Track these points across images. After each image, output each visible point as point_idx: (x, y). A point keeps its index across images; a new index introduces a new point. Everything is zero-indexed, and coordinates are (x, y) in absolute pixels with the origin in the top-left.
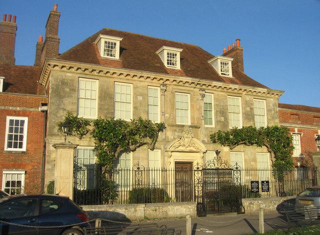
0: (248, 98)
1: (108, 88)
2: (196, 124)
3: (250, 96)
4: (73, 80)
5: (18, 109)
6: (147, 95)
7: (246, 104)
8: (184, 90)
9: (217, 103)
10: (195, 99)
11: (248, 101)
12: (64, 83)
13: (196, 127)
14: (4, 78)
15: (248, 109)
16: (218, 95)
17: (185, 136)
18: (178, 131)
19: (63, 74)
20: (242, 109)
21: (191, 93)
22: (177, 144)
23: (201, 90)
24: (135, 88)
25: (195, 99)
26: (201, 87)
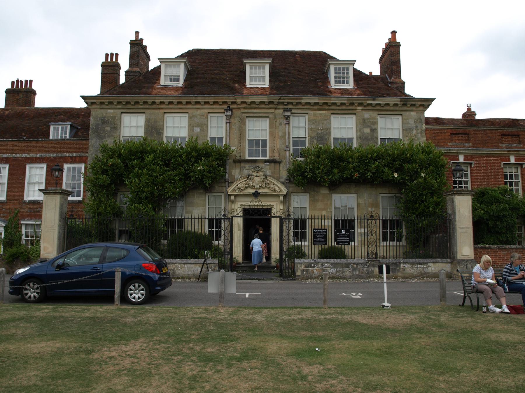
0: (367, 115)
1: (155, 122)
2: (276, 157)
3: (371, 113)
4: (115, 117)
5: (75, 155)
6: (206, 125)
7: (363, 123)
8: (259, 113)
9: (312, 126)
10: (277, 124)
11: (368, 119)
12: (104, 121)
14: (70, 123)
15: (367, 131)
16: (314, 115)
17: (255, 174)
18: (247, 167)
19: (103, 111)
20: (357, 131)
21: (271, 116)
22: (242, 185)
23: (285, 110)
24: (190, 118)
25: (277, 124)
26: (286, 107)
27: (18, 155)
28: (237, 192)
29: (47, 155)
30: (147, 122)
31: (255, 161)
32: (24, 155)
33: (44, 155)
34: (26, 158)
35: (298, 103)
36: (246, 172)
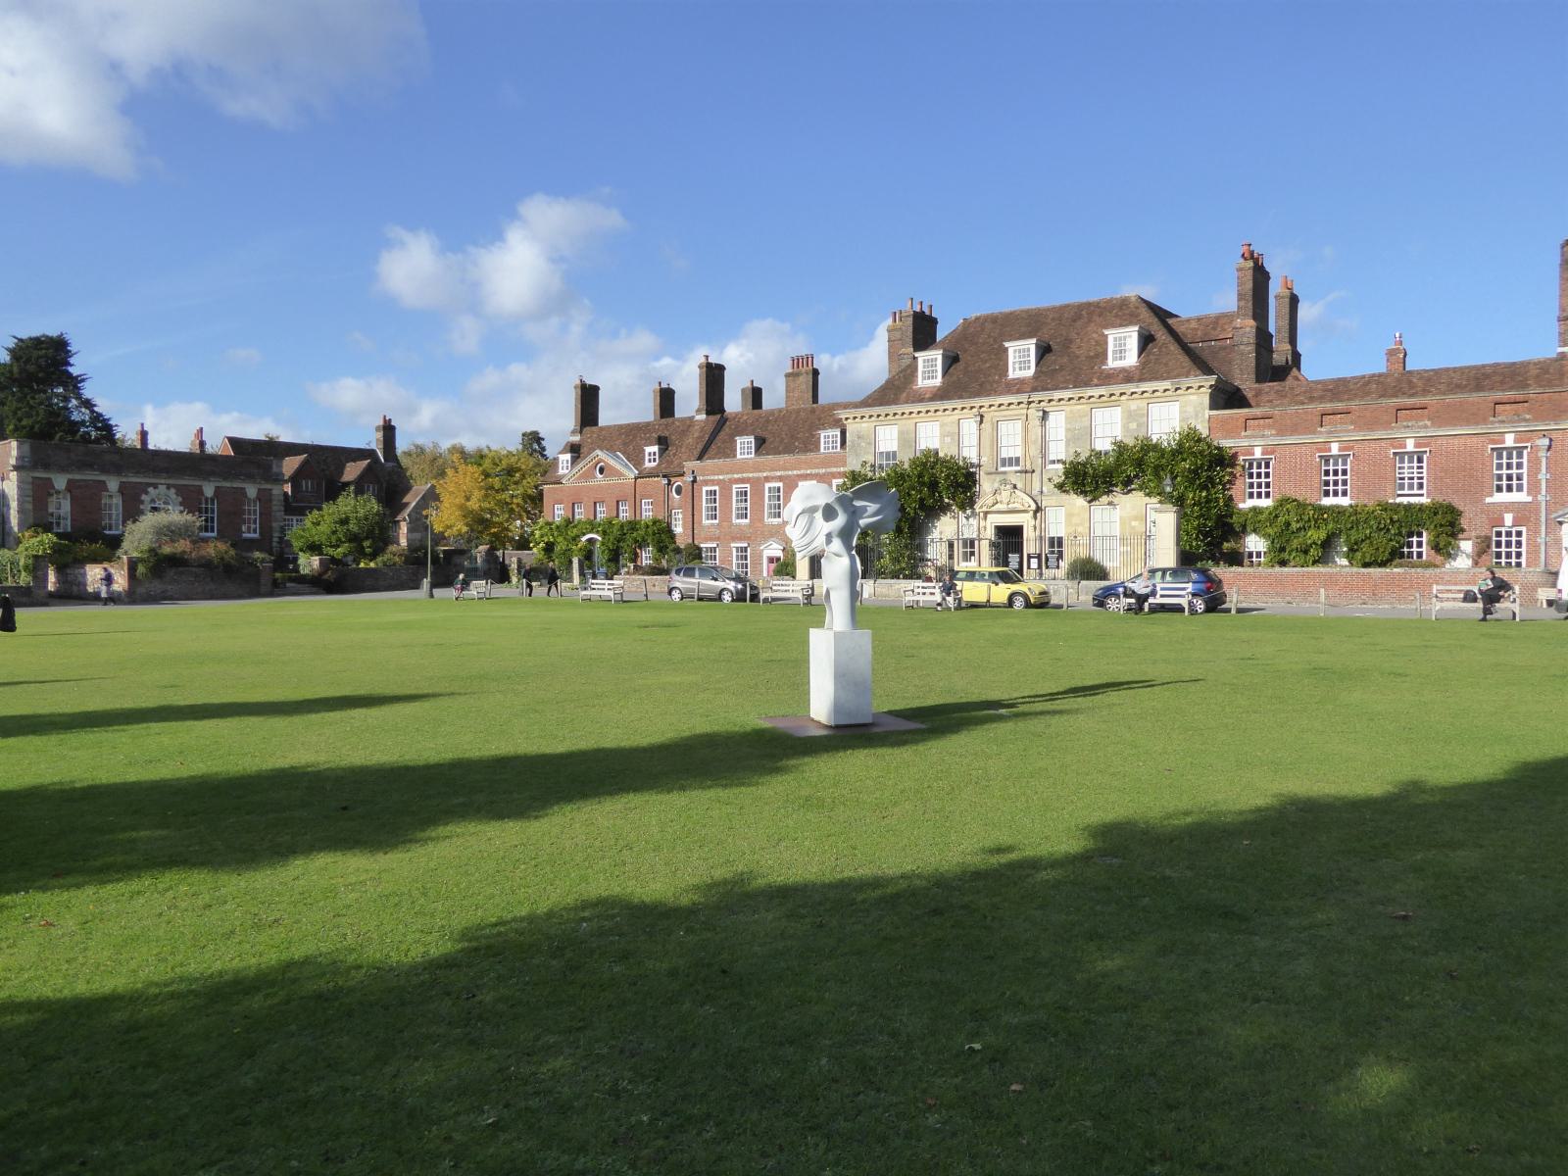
0: (1134, 405)
3: (1139, 401)
7: (1130, 416)
8: (1011, 415)
9: (1069, 426)
11: (1135, 411)
13: (1026, 472)
22: (990, 502)
24: (941, 426)
27: (790, 473)
28: (984, 509)
29: (817, 471)
30: (901, 433)
31: (1005, 473)
32: (795, 472)
33: (814, 471)
34: (798, 475)
35: (1050, 401)
36: (996, 485)
